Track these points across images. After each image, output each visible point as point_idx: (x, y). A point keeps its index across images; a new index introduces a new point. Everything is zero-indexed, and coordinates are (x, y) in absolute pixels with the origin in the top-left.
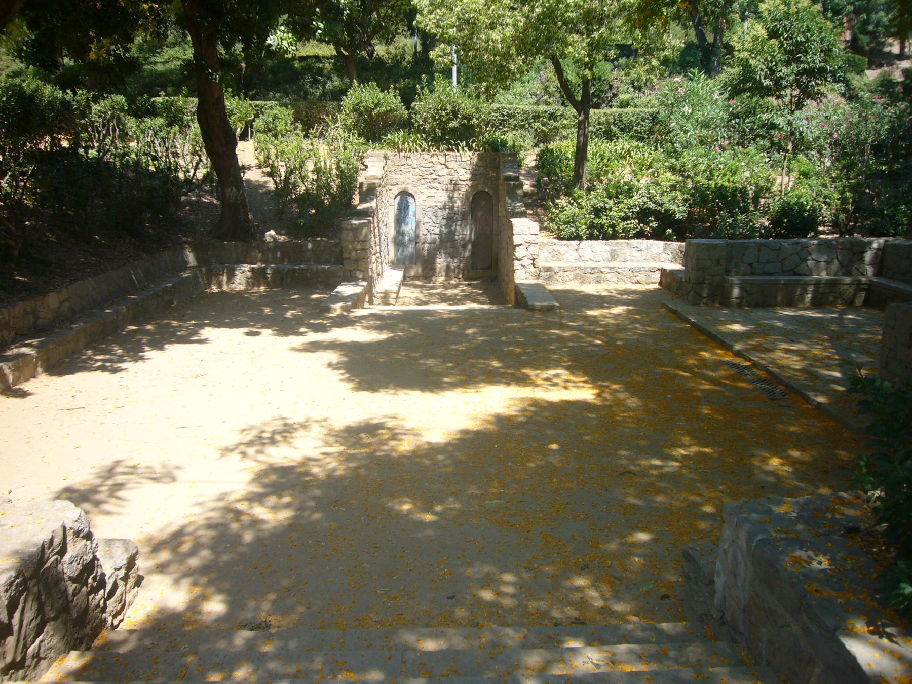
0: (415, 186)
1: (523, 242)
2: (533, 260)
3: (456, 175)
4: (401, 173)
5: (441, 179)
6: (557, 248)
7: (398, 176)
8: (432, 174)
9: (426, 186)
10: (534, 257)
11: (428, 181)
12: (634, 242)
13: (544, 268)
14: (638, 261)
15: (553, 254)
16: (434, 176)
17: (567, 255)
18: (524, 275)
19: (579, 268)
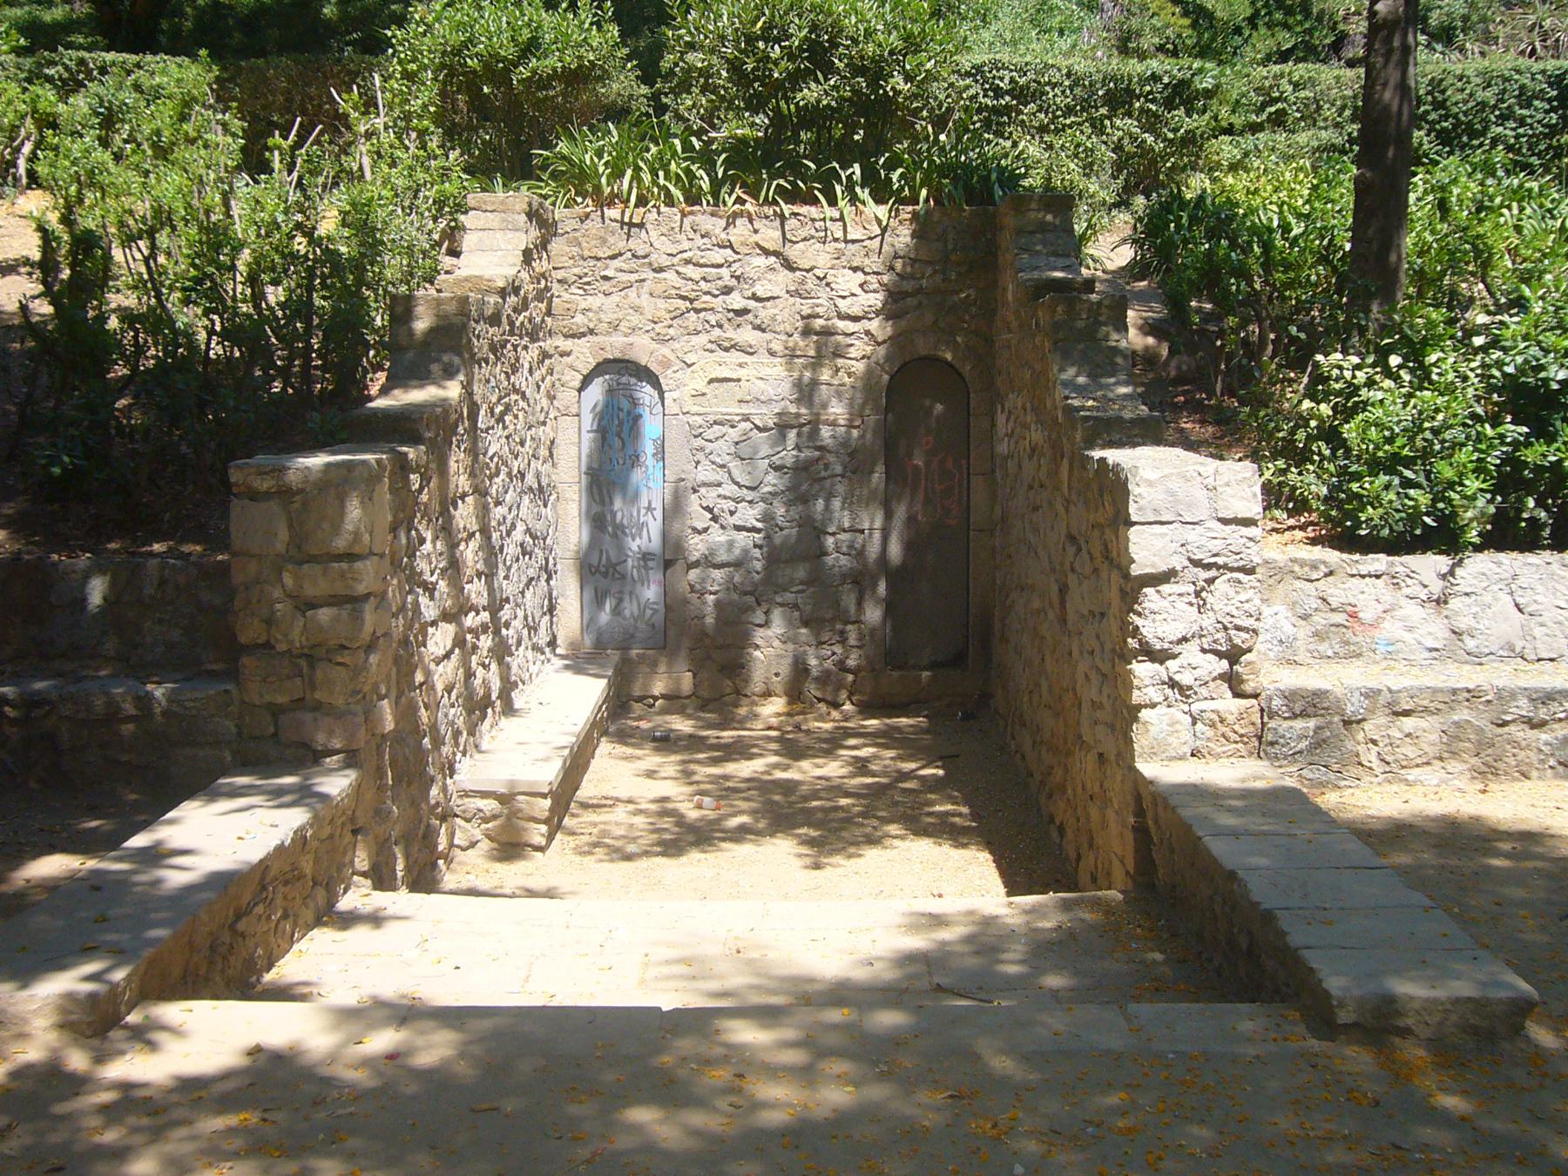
0: (663, 340)
1: (1178, 562)
2: (1233, 655)
3: (824, 294)
4: (606, 286)
5: (764, 313)
6: (1339, 591)
7: (595, 302)
8: (727, 291)
9: (703, 339)
10: (1239, 638)
13: (1290, 696)
15: (1320, 620)
16: (736, 300)
17: (1391, 629)
18: (1183, 738)
19: (1473, 694)
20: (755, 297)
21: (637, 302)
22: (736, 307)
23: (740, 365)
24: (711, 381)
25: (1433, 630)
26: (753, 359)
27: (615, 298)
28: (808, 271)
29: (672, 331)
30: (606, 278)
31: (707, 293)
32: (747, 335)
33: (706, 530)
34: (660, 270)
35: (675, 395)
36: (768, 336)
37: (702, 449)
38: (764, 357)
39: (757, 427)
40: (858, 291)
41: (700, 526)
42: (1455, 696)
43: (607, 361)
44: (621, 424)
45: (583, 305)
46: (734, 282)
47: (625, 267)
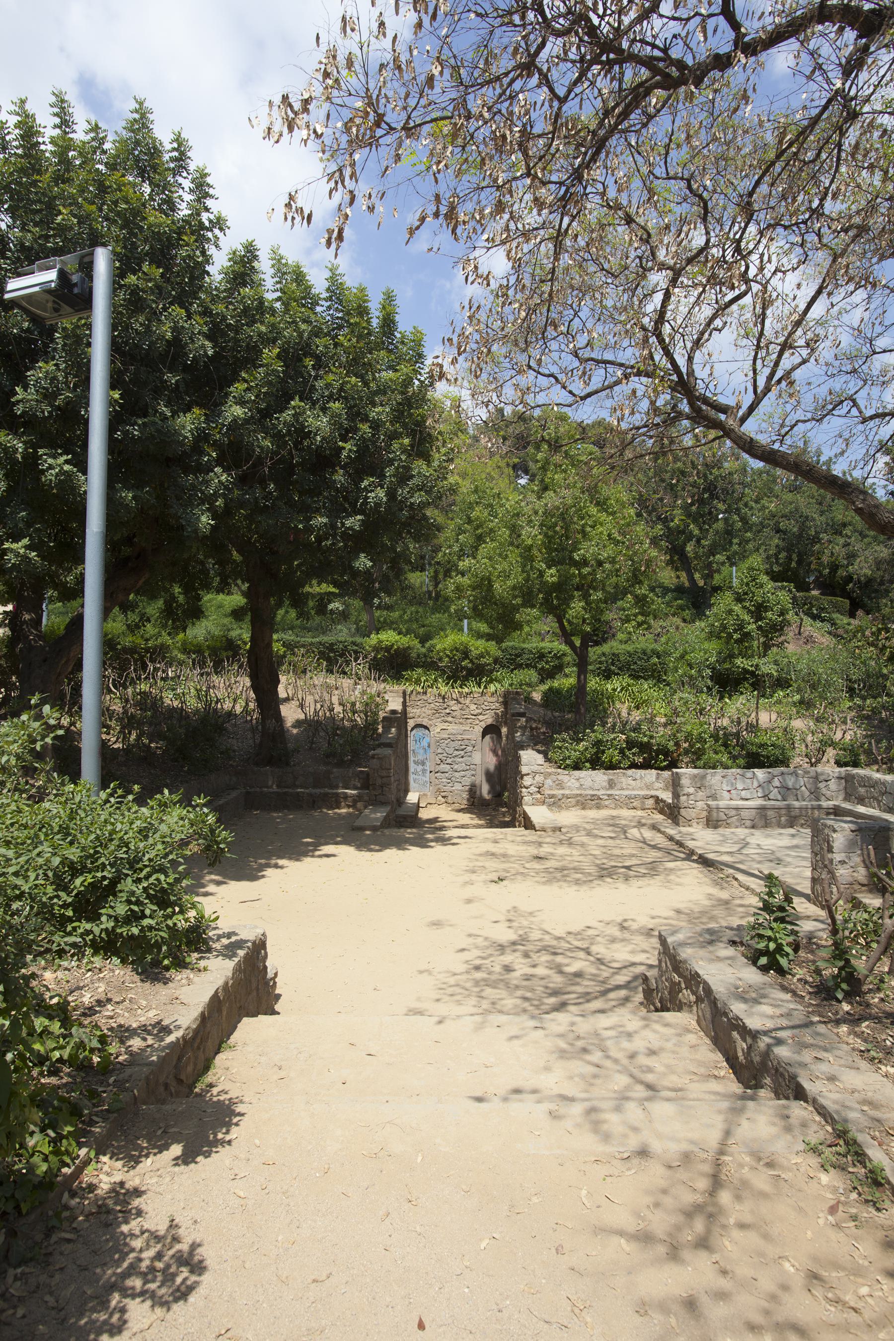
5: (454, 714)
6: (560, 777)
12: (630, 772)
14: (633, 789)
16: (447, 711)
18: (531, 802)
25: (577, 785)
32: (450, 719)
42: (577, 795)
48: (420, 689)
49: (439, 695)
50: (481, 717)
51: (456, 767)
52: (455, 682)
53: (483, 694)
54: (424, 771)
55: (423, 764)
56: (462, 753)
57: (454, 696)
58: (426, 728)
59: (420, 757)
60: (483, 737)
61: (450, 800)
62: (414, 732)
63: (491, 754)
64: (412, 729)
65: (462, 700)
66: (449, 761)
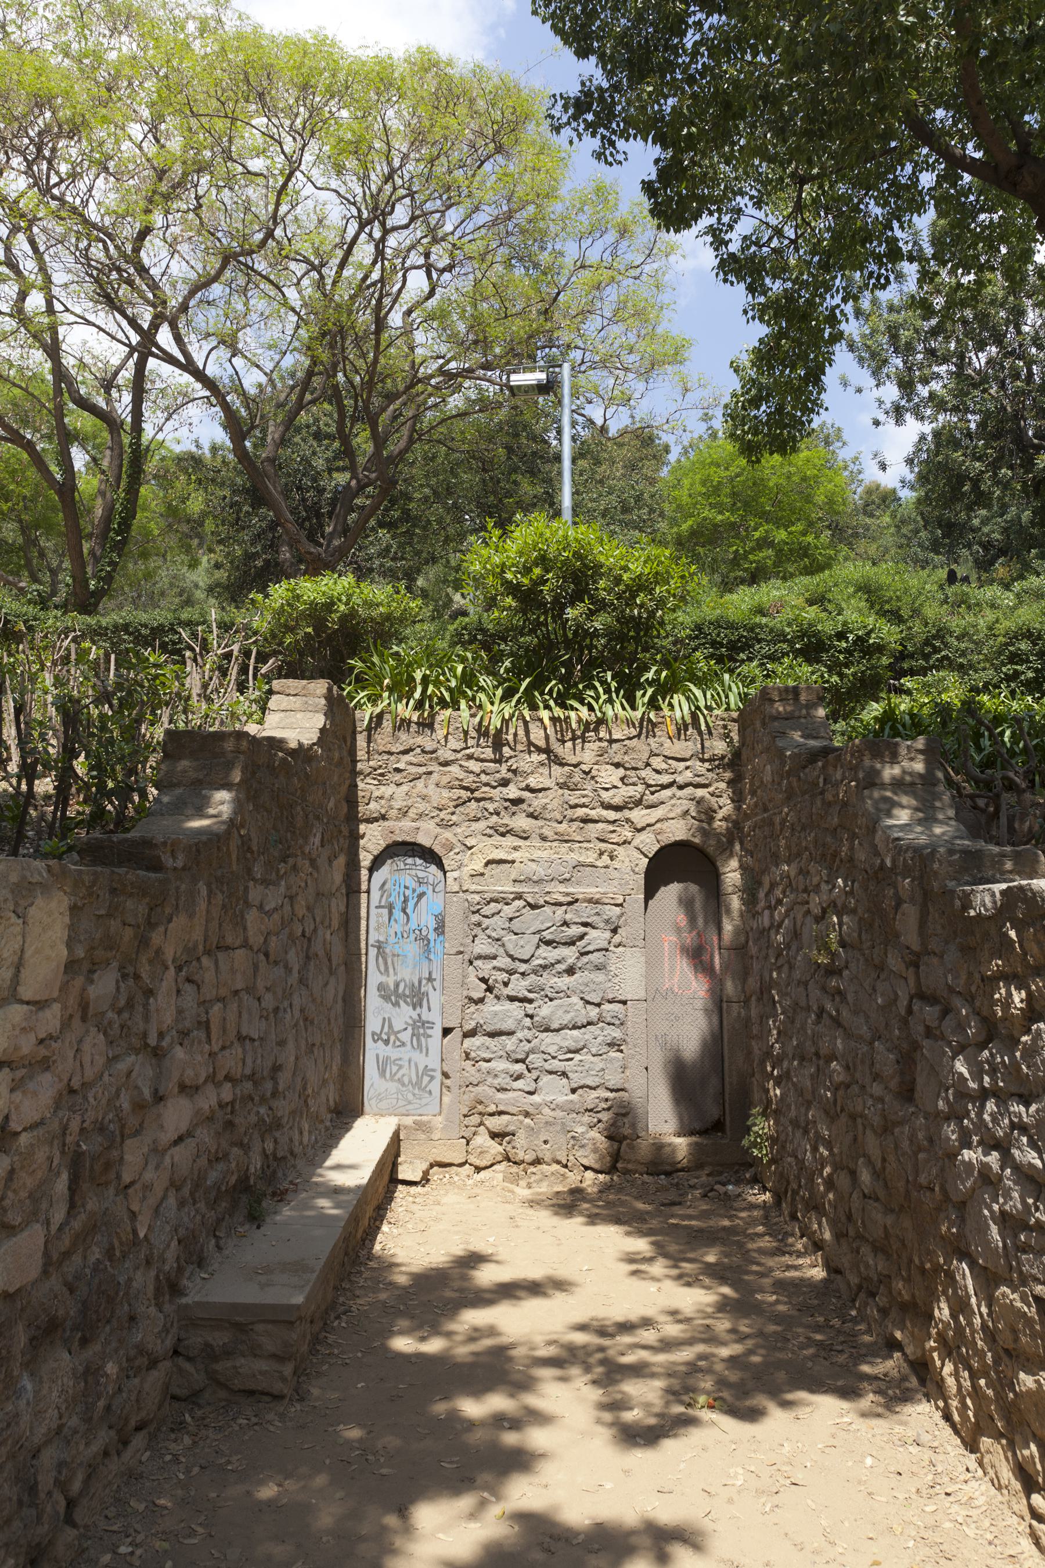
3: (589, 785)
4: (397, 777)
5: (537, 802)
7: (387, 791)
8: (505, 783)
9: (482, 825)
11: (491, 807)
20: (528, 789)
21: (425, 791)
22: (511, 796)
23: (515, 849)
24: (488, 863)
26: (527, 843)
27: (405, 788)
28: (575, 766)
29: (454, 818)
30: (398, 770)
31: (487, 784)
32: (521, 822)
33: (481, 1000)
34: (446, 764)
35: (456, 874)
36: (540, 823)
37: (479, 925)
38: (536, 842)
39: (529, 905)
40: (620, 784)
41: (476, 995)
43: (396, 844)
44: (406, 901)
45: (376, 794)
46: (510, 775)
47: (415, 760)
48: (405, 710)
49: (482, 731)
50: (639, 816)
51: (545, 1011)
52: (538, 684)
53: (647, 728)
54: (420, 1026)
55: (417, 998)
56: (569, 954)
57: (537, 736)
58: (430, 856)
59: (407, 973)
60: (650, 892)
61: (522, 1147)
62: (379, 876)
63: (683, 967)
64: (377, 863)
65: (564, 751)
66: (519, 986)
